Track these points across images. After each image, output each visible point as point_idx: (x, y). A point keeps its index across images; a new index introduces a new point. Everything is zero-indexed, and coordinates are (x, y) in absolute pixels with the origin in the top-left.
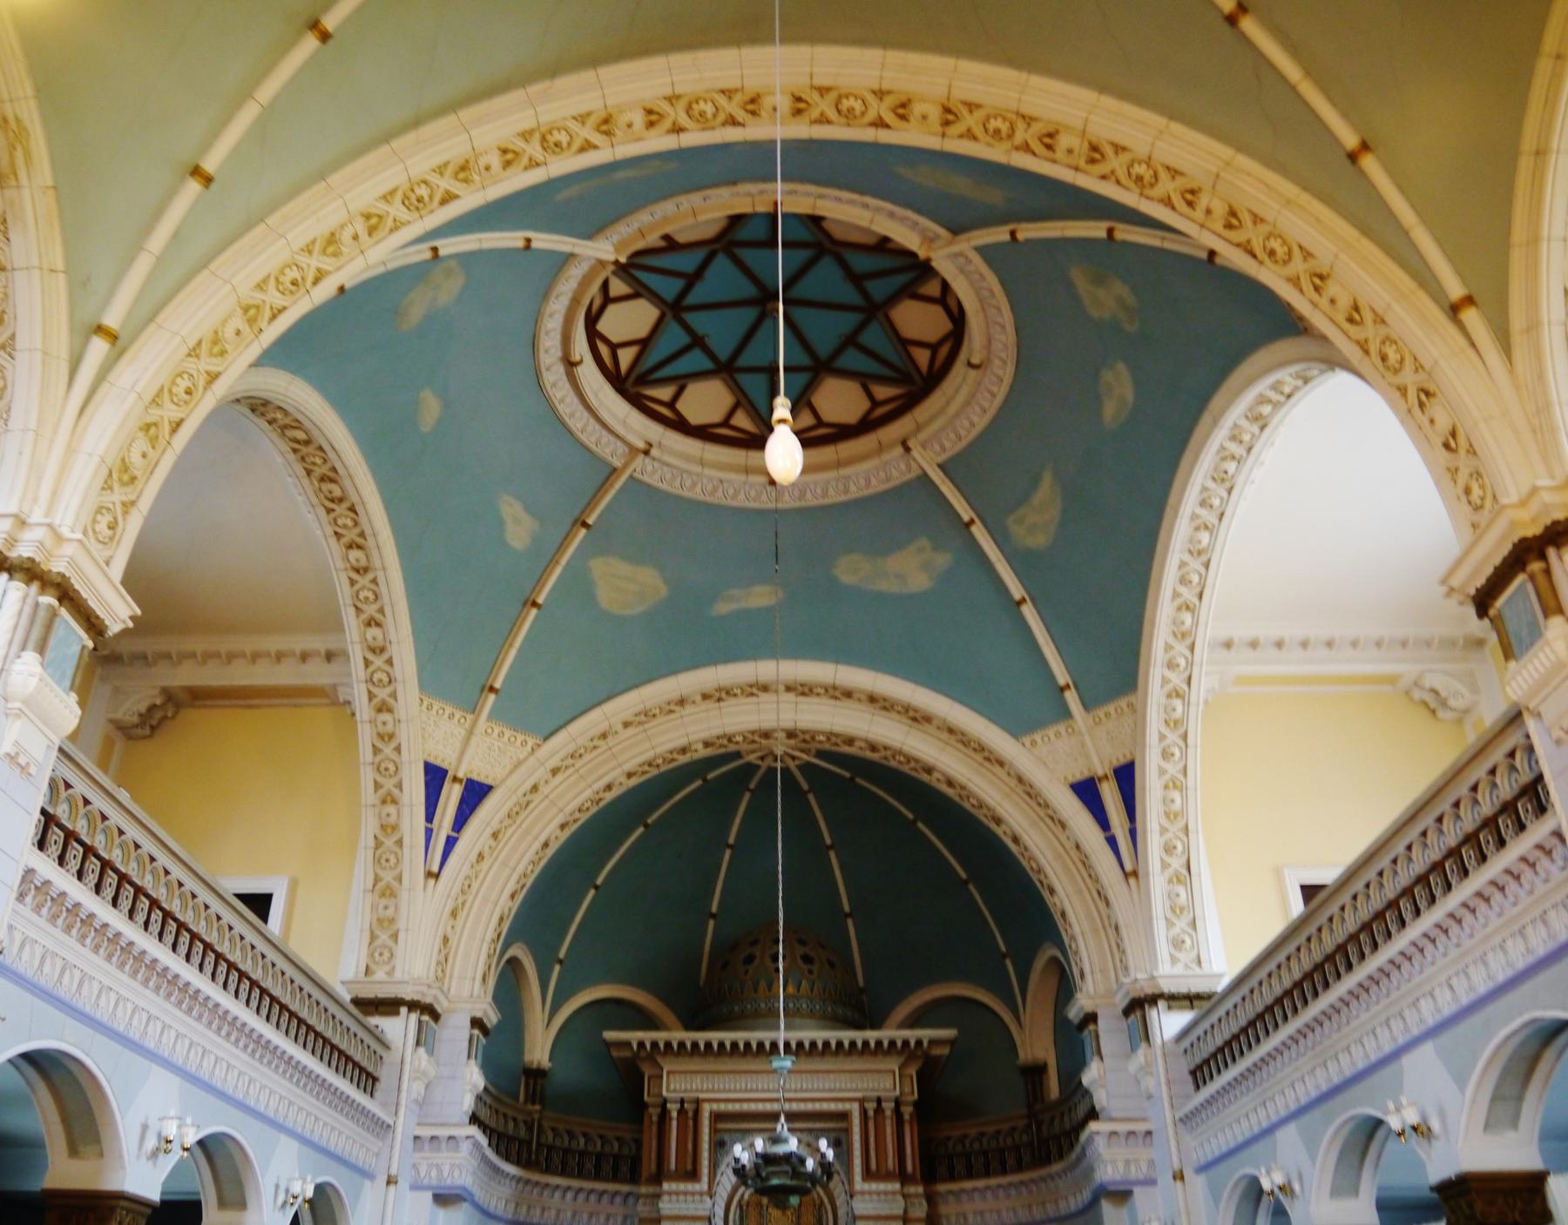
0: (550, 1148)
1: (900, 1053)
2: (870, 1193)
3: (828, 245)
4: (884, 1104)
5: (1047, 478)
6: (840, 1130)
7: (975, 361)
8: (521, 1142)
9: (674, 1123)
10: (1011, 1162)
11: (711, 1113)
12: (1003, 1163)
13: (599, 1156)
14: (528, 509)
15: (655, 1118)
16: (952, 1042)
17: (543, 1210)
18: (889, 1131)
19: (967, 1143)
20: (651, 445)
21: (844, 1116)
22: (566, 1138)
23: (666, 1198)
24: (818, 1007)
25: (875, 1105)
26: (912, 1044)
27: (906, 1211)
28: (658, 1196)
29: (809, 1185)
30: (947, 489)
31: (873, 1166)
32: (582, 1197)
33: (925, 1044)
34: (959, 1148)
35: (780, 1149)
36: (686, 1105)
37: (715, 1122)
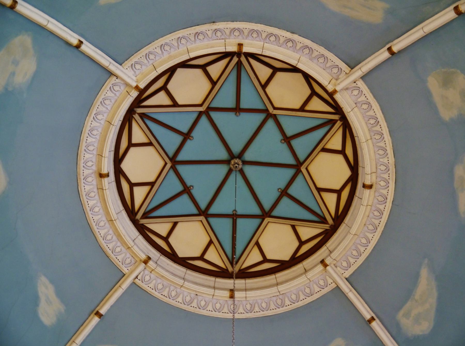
3: (271, 110)
5: (424, 273)
7: (368, 183)
14: (60, 294)
20: (149, 258)
30: (353, 296)
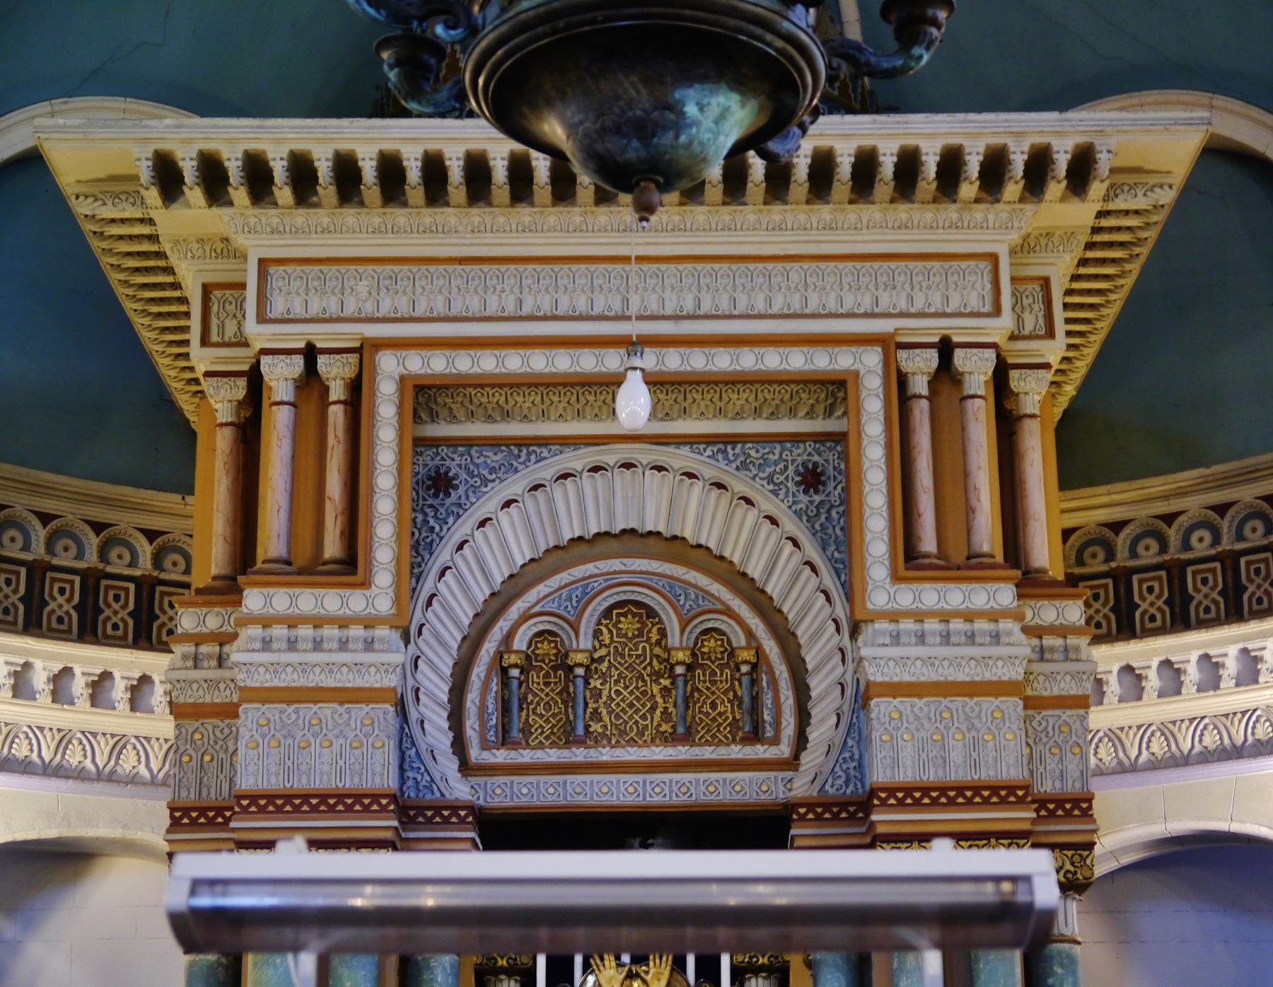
2: (919, 616)
4: (960, 358)
6: (821, 438)
19: (1173, 534)
25: (930, 360)
31: (928, 543)
34: (1149, 554)
36: (322, 360)
37: (417, 418)
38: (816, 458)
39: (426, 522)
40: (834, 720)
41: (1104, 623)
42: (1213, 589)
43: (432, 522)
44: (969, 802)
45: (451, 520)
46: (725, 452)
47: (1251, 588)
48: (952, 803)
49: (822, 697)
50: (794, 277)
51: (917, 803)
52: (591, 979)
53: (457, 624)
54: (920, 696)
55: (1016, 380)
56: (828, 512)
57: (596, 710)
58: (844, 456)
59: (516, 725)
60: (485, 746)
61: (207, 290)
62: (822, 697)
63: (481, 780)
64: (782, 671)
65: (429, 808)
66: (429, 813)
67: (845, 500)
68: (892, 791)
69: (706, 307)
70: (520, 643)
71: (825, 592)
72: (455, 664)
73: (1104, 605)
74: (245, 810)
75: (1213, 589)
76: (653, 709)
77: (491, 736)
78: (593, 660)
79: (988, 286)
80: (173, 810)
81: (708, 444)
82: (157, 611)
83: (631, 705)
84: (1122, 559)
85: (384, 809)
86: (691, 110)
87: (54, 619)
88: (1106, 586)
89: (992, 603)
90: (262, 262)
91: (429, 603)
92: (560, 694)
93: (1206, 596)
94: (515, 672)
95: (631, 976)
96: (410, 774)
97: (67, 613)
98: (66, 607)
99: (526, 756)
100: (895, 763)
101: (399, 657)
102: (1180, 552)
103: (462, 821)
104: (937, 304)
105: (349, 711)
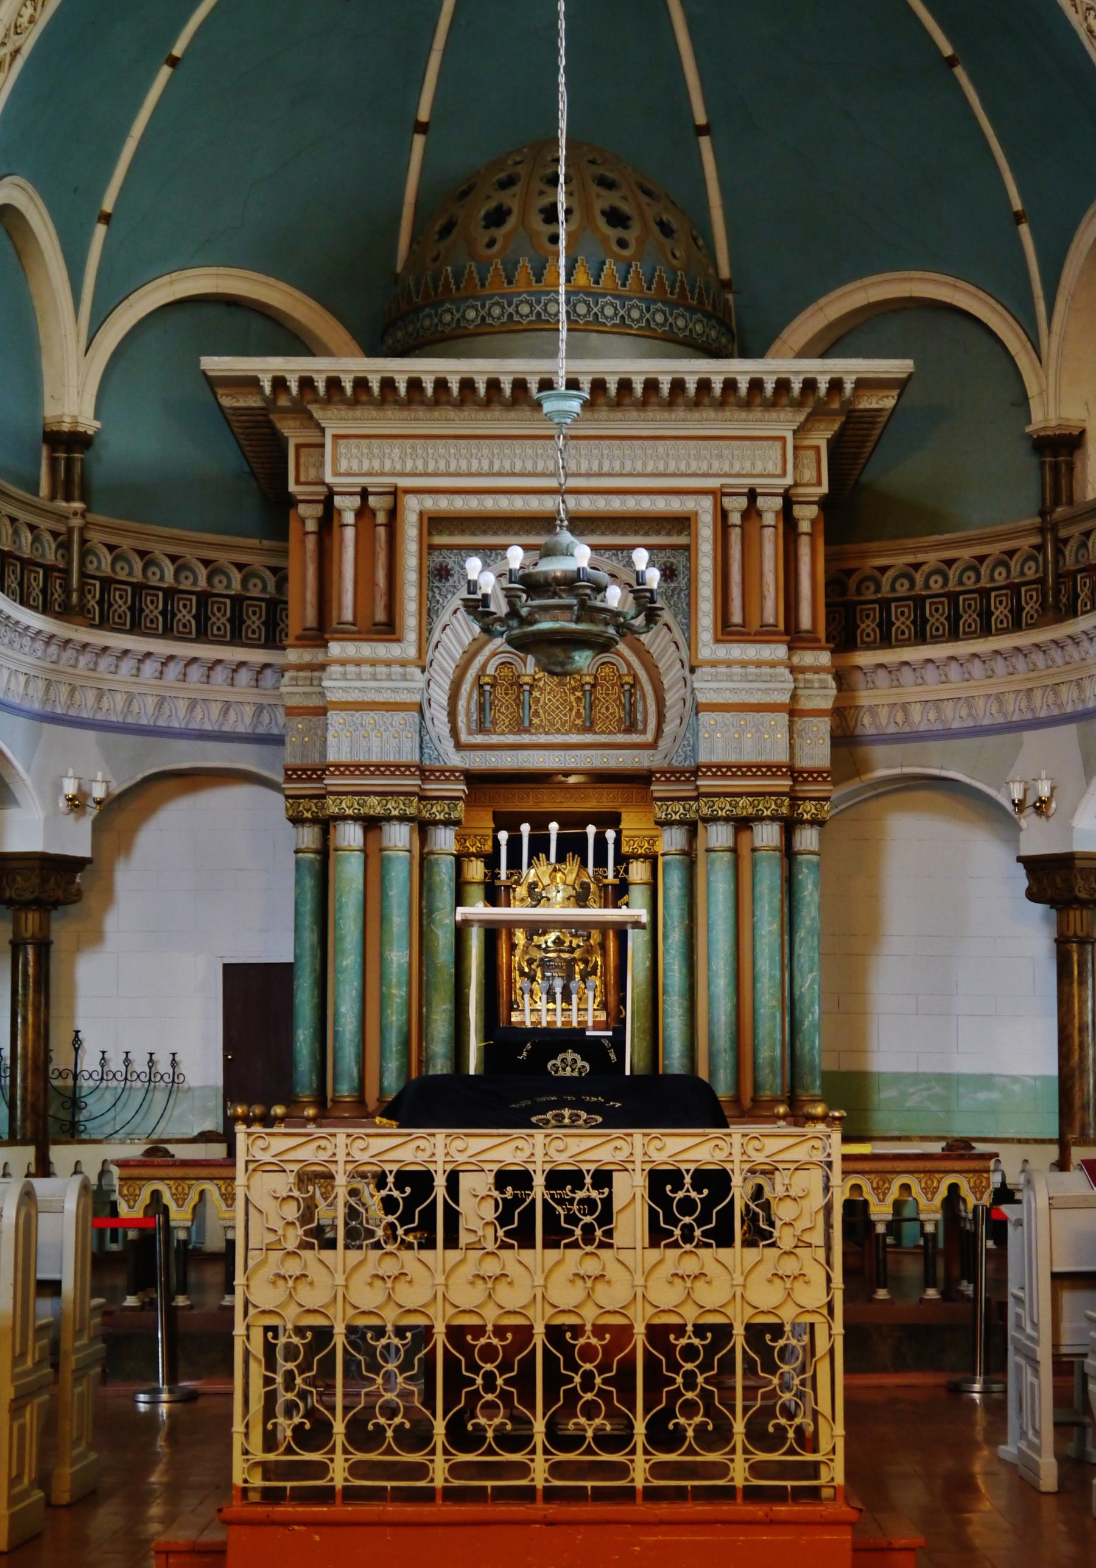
0: (107, 583)
1: (798, 404)
2: (729, 664)
4: (761, 502)
8: (48, 569)
9: (349, 533)
10: (1000, 612)
11: (421, 514)
12: (985, 615)
13: (203, 598)
15: (311, 526)
16: (902, 385)
17: (100, 693)
18: (769, 550)
19: (919, 578)
21: (683, 523)
22: (138, 564)
23: (335, 669)
24: (635, 314)
25: (743, 502)
26: (823, 387)
27: (794, 697)
28: (322, 667)
29: (611, 631)
31: (736, 618)
32: (173, 671)
33: (849, 387)
34: (903, 589)
35: (556, 566)
37: (430, 534)
38: (672, 560)
39: (434, 597)
40: (679, 721)
41: (872, 634)
42: (942, 615)
43: (438, 597)
44: (754, 775)
45: (449, 596)
46: (617, 555)
47: (965, 617)
48: (744, 775)
49: (672, 706)
50: (661, 450)
51: (724, 775)
52: (533, 871)
53: (453, 659)
54: (728, 712)
55: (798, 511)
56: (679, 594)
57: (536, 710)
58: (689, 559)
59: (488, 719)
60: (470, 733)
61: (298, 447)
62: (672, 706)
63: (467, 753)
64: (648, 689)
65: (437, 771)
66: (437, 774)
67: (689, 587)
68: (709, 767)
69: (605, 469)
70: (490, 670)
71: (675, 643)
72: (452, 682)
73: (873, 622)
74: (332, 774)
75: (942, 615)
76: (571, 710)
77: (473, 726)
78: (534, 680)
79: (780, 457)
80: (286, 770)
81: (607, 550)
82: (245, 618)
83: (558, 708)
84: (885, 591)
85: (413, 774)
86: (577, 658)
87: (181, 625)
88: (874, 609)
89: (773, 656)
90: (336, 437)
91: (436, 647)
92: (514, 700)
93: (937, 620)
94: (487, 688)
95: (555, 870)
96: (426, 750)
97: (189, 621)
98: (188, 617)
99: (494, 739)
100: (712, 751)
101: (422, 685)
102: (922, 590)
103: (457, 779)
104: (747, 467)
105: (392, 716)
